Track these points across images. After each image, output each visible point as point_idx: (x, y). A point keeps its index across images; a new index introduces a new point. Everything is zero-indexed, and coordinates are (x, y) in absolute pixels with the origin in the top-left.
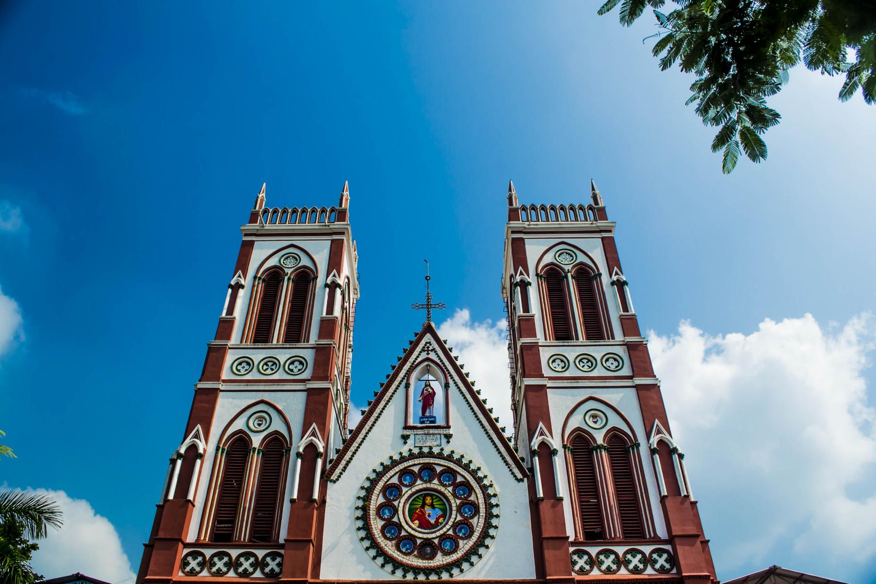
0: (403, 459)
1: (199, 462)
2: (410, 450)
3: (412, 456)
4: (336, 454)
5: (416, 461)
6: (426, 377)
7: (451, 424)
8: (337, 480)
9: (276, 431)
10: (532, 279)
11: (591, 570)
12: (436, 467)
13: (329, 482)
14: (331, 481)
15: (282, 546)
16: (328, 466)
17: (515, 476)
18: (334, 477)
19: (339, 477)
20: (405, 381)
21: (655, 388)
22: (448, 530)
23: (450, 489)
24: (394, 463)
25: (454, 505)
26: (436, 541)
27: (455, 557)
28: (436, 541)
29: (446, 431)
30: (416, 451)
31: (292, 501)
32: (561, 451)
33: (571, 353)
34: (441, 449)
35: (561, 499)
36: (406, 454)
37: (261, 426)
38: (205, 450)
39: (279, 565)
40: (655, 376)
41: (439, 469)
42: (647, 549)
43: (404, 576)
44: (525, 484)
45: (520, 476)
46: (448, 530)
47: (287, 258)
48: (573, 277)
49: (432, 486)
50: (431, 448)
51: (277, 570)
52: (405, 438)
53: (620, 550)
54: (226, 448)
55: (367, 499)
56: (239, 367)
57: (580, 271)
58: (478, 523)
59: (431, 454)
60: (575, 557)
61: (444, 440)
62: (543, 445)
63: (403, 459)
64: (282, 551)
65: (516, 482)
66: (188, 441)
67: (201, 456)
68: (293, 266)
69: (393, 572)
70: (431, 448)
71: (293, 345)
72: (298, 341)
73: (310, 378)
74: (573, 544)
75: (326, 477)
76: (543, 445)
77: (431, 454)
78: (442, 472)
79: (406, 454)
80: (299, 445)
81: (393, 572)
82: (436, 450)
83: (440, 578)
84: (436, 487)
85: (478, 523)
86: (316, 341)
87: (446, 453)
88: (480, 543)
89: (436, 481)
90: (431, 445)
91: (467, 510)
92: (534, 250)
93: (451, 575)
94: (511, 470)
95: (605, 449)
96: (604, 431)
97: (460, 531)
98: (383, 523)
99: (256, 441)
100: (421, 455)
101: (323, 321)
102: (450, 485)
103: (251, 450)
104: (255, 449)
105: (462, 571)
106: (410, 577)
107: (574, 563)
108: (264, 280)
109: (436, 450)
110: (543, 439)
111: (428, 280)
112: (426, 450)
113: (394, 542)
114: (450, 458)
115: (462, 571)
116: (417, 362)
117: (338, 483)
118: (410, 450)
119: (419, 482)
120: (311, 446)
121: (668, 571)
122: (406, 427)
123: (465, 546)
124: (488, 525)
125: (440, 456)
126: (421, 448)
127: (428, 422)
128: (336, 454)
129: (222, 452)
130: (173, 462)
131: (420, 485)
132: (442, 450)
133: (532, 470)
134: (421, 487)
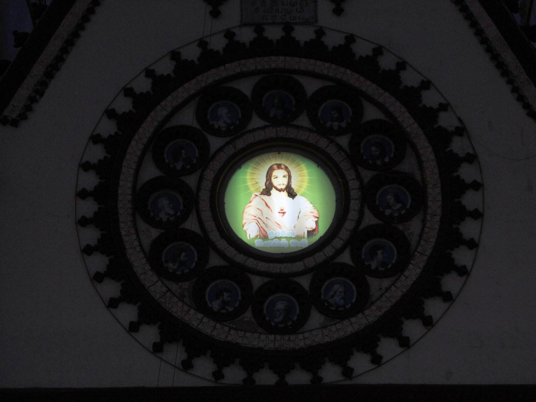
2: (229, 34)
4: (16, 46)
5: (251, 64)
8: (23, 117)
12: (303, 80)
19: (28, 108)
22: (339, 252)
23: (344, 141)
25: (353, 184)
26: (305, 282)
34: (316, 32)
43: (218, 375)
46: (339, 252)
50: (288, 28)
69: (187, 366)
81: (187, 366)
89: (303, 121)
91: (390, 198)
93: (348, 372)
94: (515, 90)
98: (155, 233)
102: (341, 132)
105: (377, 360)
113: (186, 285)
115: (377, 360)
119: (256, 122)
128: (16, 46)
132: (320, 32)
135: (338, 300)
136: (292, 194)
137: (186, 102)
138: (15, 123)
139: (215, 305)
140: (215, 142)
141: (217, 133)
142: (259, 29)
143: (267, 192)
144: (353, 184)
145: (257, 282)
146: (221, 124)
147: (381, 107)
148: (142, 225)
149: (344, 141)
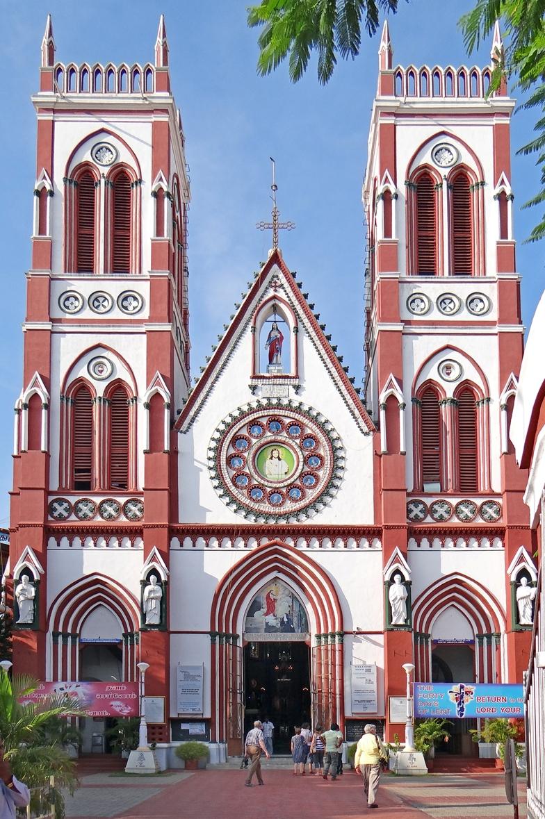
0: (252, 411)
1: (44, 412)
3: (260, 408)
5: (266, 413)
6: (272, 318)
7: (299, 374)
9: (119, 378)
10: (402, 189)
11: (425, 518)
13: (179, 433)
14: (181, 432)
15: (141, 494)
16: (177, 417)
17: (361, 430)
18: (184, 428)
20: (251, 324)
21: (522, 338)
24: (243, 415)
26: (284, 490)
27: (302, 504)
28: (284, 490)
29: (296, 382)
30: (264, 402)
31: (145, 452)
32: (410, 404)
33: (431, 289)
35: (404, 454)
36: (254, 405)
37: (103, 373)
38: (49, 400)
39: (141, 510)
40: (520, 322)
41: (287, 421)
42: (479, 501)
44: (370, 438)
45: (366, 429)
47: (99, 150)
48: (449, 187)
49: (279, 438)
51: (138, 513)
52: (254, 388)
53: (454, 501)
54: (70, 396)
55: (218, 450)
56: (67, 303)
57: (459, 177)
58: (324, 474)
59: (279, 406)
60: (411, 506)
61: (292, 391)
62: (392, 398)
63: (252, 411)
64: (142, 499)
65: (363, 435)
66: (28, 391)
67: (47, 407)
68: (108, 163)
70: (279, 399)
71: (124, 276)
72: (127, 271)
73: (147, 318)
74: (409, 495)
75: (175, 427)
76: (392, 398)
77: (279, 406)
78: (291, 425)
79: (254, 405)
80: (144, 396)
82: (285, 402)
83: (288, 522)
84: (284, 439)
85: (324, 474)
86: (149, 272)
87: (295, 404)
88: (326, 492)
90: (278, 396)
92: (410, 137)
95: (454, 403)
96: (457, 383)
97: (307, 480)
99: (99, 388)
100: (269, 406)
101: (155, 246)
102: (296, 438)
103: (95, 399)
104: (100, 397)
106: (262, 521)
107: (409, 511)
108: (76, 184)
109: (285, 402)
110: (392, 392)
111: (276, 186)
112: (274, 401)
114: (298, 410)
116: (262, 303)
117: (188, 433)
118: (258, 401)
120: (156, 397)
121: (496, 521)
122: (255, 377)
123: (311, 494)
124: (334, 476)
125: (289, 407)
126: (269, 399)
127: (276, 371)
129: (67, 401)
130: (19, 411)
131: (269, 436)
132: (290, 401)
133: (378, 424)
134: (269, 439)
135: (295, 496)
136: (279, 459)
137: (244, 425)
138: (185, 433)
139: (254, 497)
140: (254, 441)
141: (254, 437)
142: (269, 399)
143: (271, 458)
144: (301, 457)
145: (269, 489)
146: (255, 434)
147: (311, 429)
148: (229, 470)
149: (298, 441)
